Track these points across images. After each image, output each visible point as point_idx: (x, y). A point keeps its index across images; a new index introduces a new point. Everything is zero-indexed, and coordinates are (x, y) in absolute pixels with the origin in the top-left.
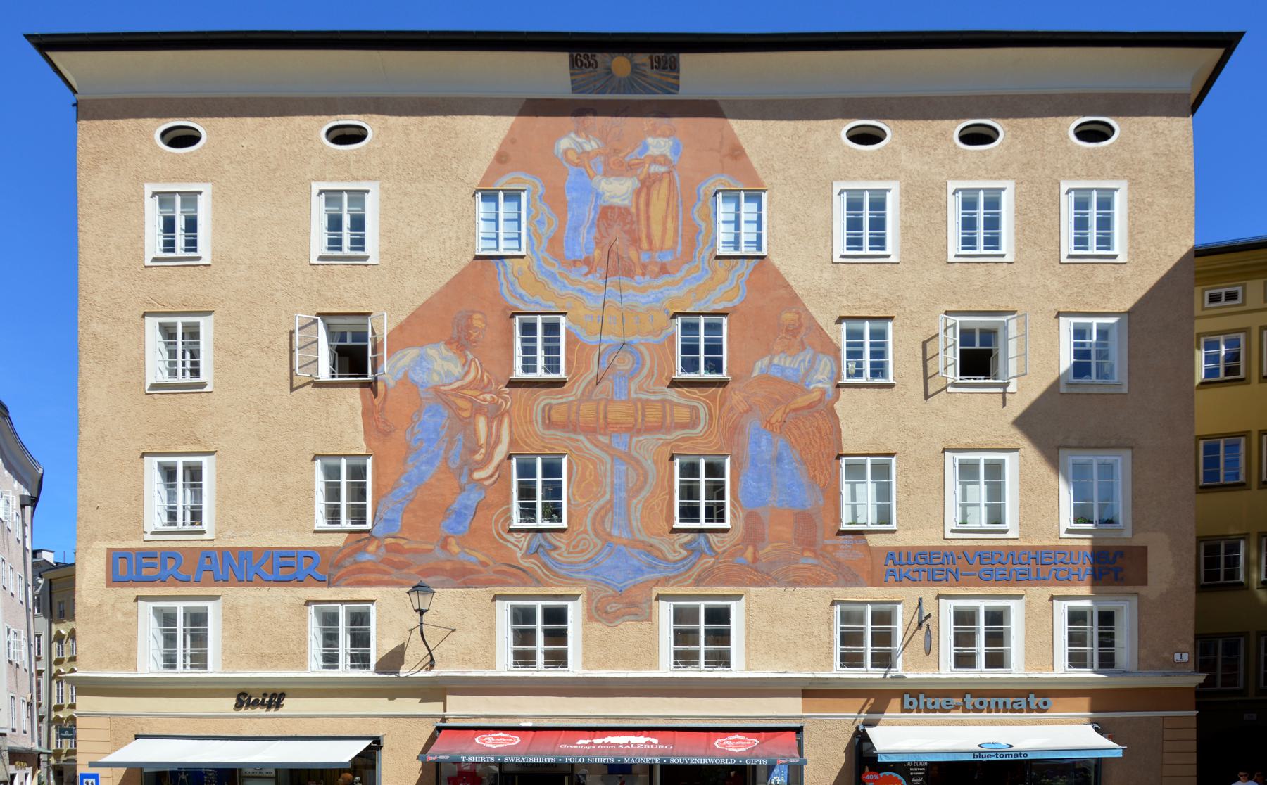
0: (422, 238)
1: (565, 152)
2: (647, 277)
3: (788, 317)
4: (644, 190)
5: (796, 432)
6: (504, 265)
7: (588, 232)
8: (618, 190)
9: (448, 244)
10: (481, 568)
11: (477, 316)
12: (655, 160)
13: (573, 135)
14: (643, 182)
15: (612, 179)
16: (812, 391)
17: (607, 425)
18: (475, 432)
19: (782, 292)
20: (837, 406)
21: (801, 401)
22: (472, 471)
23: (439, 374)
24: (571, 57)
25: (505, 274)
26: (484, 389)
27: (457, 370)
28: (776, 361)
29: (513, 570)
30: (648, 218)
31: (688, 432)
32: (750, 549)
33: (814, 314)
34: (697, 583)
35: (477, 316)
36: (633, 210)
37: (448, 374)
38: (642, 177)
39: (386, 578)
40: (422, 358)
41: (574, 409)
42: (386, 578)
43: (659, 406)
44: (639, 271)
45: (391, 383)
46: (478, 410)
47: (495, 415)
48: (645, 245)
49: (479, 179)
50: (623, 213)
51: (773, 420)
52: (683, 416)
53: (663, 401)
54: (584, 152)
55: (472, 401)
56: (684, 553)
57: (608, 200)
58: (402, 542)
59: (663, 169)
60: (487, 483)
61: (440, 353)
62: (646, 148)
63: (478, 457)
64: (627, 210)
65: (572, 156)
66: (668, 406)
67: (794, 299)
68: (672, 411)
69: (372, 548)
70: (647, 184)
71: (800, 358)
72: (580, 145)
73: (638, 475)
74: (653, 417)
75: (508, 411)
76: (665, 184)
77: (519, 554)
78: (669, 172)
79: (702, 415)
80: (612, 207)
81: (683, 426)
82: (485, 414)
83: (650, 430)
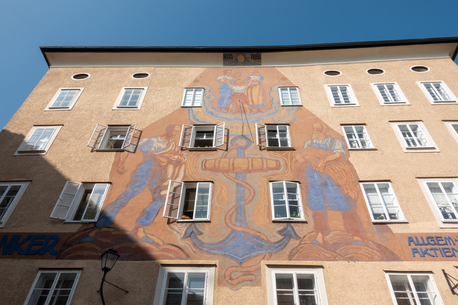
0: (160, 102)
1: (220, 79)
2: (252, 113)
3: (316, 125)
5: (332, 171)
6: (192, 110)
7: (228, 100)
9: (170, 104)
11: (177, 126)
12: (253, 81)
16: (335, 153)
17: (234, 168)
18: (166, 172)
19: (311, 117)
20: (350, 159)
21: (331, 158)
22: (161, 191)
23: (155, 148)
25: (192, 113)
26: (175, 154)
28: (314, 141)
29: (173, 248)
30: (252, 96)
31: (276, 172)
32: (320, 235)
34: (290, 257)
36: (246, 94)
39: (94, 253)
41: (218, 161)
42: (94, 253)
43: (260, 160)
47: (178, 164)
48: (251, 103)
50: (241, 95)
51: (319, 166)
52: (273, 164)
53: (262, 158)
54: (227, 79)
56: (280, 237)
62: (250, 78)
64: (243, 94)
65: (223, 80)
66: (264, 160)
67: (317, 120)
68: (266, 162)
69: (92, 234)
71: (326, 140)
74: (257, 164)
75: (185, 163)
77: (179, 237)
79: (282, 164)
80: (237, 93)
81: (273, 169)
82: (173, 164)
83: (256, 170)
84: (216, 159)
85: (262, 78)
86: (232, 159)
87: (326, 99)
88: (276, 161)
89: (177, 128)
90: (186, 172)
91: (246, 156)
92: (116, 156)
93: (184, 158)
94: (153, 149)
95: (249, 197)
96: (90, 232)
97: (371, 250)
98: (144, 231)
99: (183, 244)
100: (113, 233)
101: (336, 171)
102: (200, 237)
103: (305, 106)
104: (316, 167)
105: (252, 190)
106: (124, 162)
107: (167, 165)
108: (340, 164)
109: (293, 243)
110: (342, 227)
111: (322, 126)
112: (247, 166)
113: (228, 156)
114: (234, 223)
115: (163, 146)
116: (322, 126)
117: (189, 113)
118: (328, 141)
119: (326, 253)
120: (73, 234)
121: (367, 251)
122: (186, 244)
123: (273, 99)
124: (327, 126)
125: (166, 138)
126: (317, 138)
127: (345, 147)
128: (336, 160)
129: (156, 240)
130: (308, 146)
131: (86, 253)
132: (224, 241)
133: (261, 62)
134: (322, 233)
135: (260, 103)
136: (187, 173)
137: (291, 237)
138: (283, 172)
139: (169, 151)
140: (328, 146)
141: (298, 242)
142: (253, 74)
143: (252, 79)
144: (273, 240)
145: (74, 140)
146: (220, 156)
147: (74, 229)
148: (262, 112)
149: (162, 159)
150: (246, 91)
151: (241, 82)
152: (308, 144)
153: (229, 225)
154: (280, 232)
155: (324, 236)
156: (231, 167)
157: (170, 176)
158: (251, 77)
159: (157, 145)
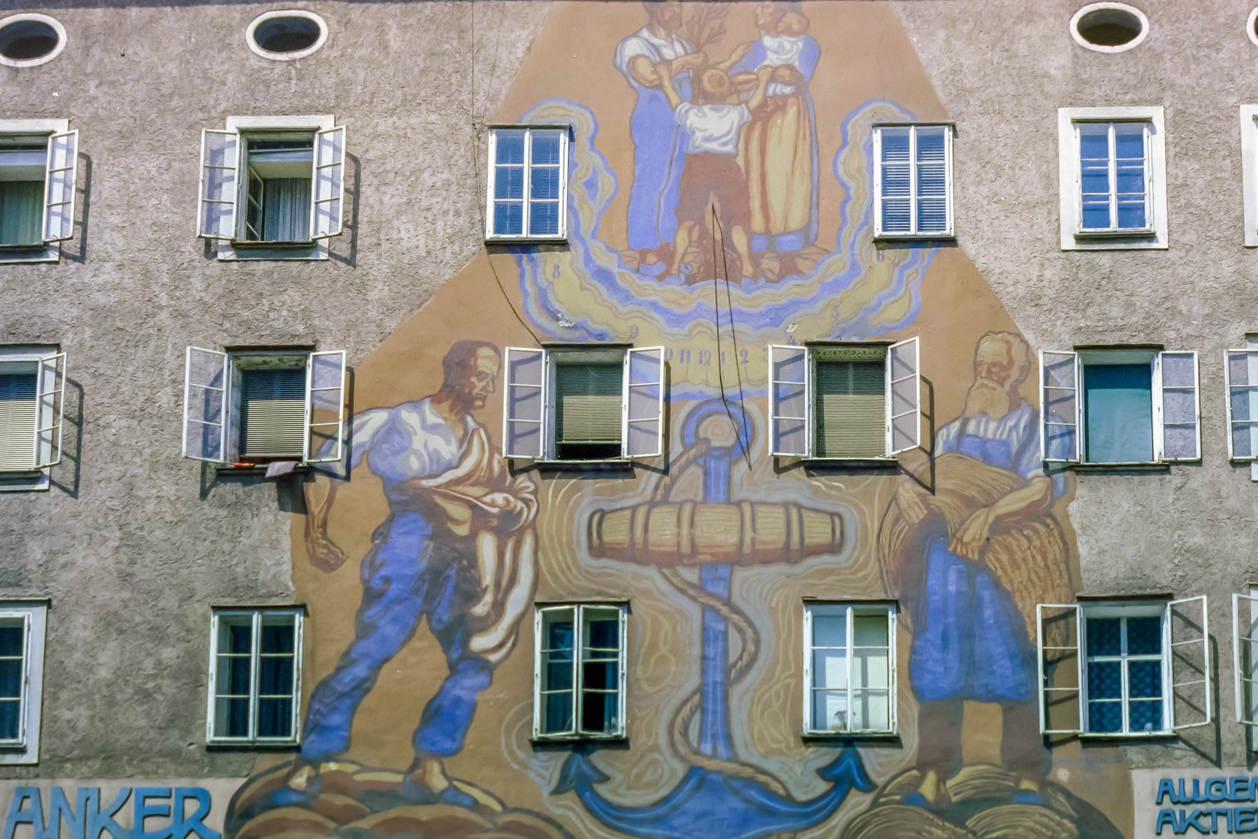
1: (633, 60)
2: (761, 281)
3: (991, 349)
4: (759, 124)
8: (713, 127)
9: (440, 224)
13: (645, 33)
15: (706, 108)
18: (474, 562)
21: (1011, 503)
26: (494, 485)
27: (448, 449)
28: (971, 428)
30: (763, 177)
32: (931, 777)
35: (484, 352)
37: (435, 456)
38: (754, 103)
40: (393, 429)
43: (780, 512)
44: (748, 269)
48: (758, 224)
51: (966, 539)
53: (786, 505)
55: (473, 507)
56: (822, 787)
57: (699, 143)
58: (350, 768)
59: (788, 90)
60: (494, 658)
63: (480, 609)
64: (726, 161)
65: (644, 68)
70: (763, 115)
71: (1011, 423)
72: (657, 49)
73: (744, 641)
75: (533, 525)
76: (792, 111)
77: (545, 793)
83: (764, 558)
84: (634, 509)
85: (813, 54)
86: (687, 509)
87: (1052, 201)
89: (484, 359)
90: (541, 562)
91: (737, 495)
93: (527, 502)
95: (741, 658)
96: (289, 776)
97: (1057, 818)
98: (443, 772)
99: (559, 811)
100: (358, 778)
101: (1019, 556)
102: (602, 790)
104: (960, 540)
105: (749, 633)
106: (324, 524)
107: (473, 536)
108: (1037, 532)
110: (995, 753)
111: (1009, 351)
112: (734, 540)
113: (673, 496)
114: (695, 744)
115: (448, 449)
116: (1009, 351)
117: (522, 276)
118: (1016, 426)
119: (938, 827)
121: (1045, 820)
123: (846, 200)
125: (452, 409)
126: (984, 413)
129: (483, 799)
134: (938, 773)
135: (796, 222)
136: (544, 569)
137: (853, 784)
138: (850, 562)
139: (468, 476)
140: (1015, 446)
141: (868, 799)
142: (774, 29)
143: (772, 59)
145: (124, 423)
146: (648, 495)
148: (799, 273)
150: (741, 146)
151: (720, 82)
152: (946, 442)
153: (682, 749)
154: (823, 773)
155: (941, 780)
158: (768, 41)
159: (425, 445)
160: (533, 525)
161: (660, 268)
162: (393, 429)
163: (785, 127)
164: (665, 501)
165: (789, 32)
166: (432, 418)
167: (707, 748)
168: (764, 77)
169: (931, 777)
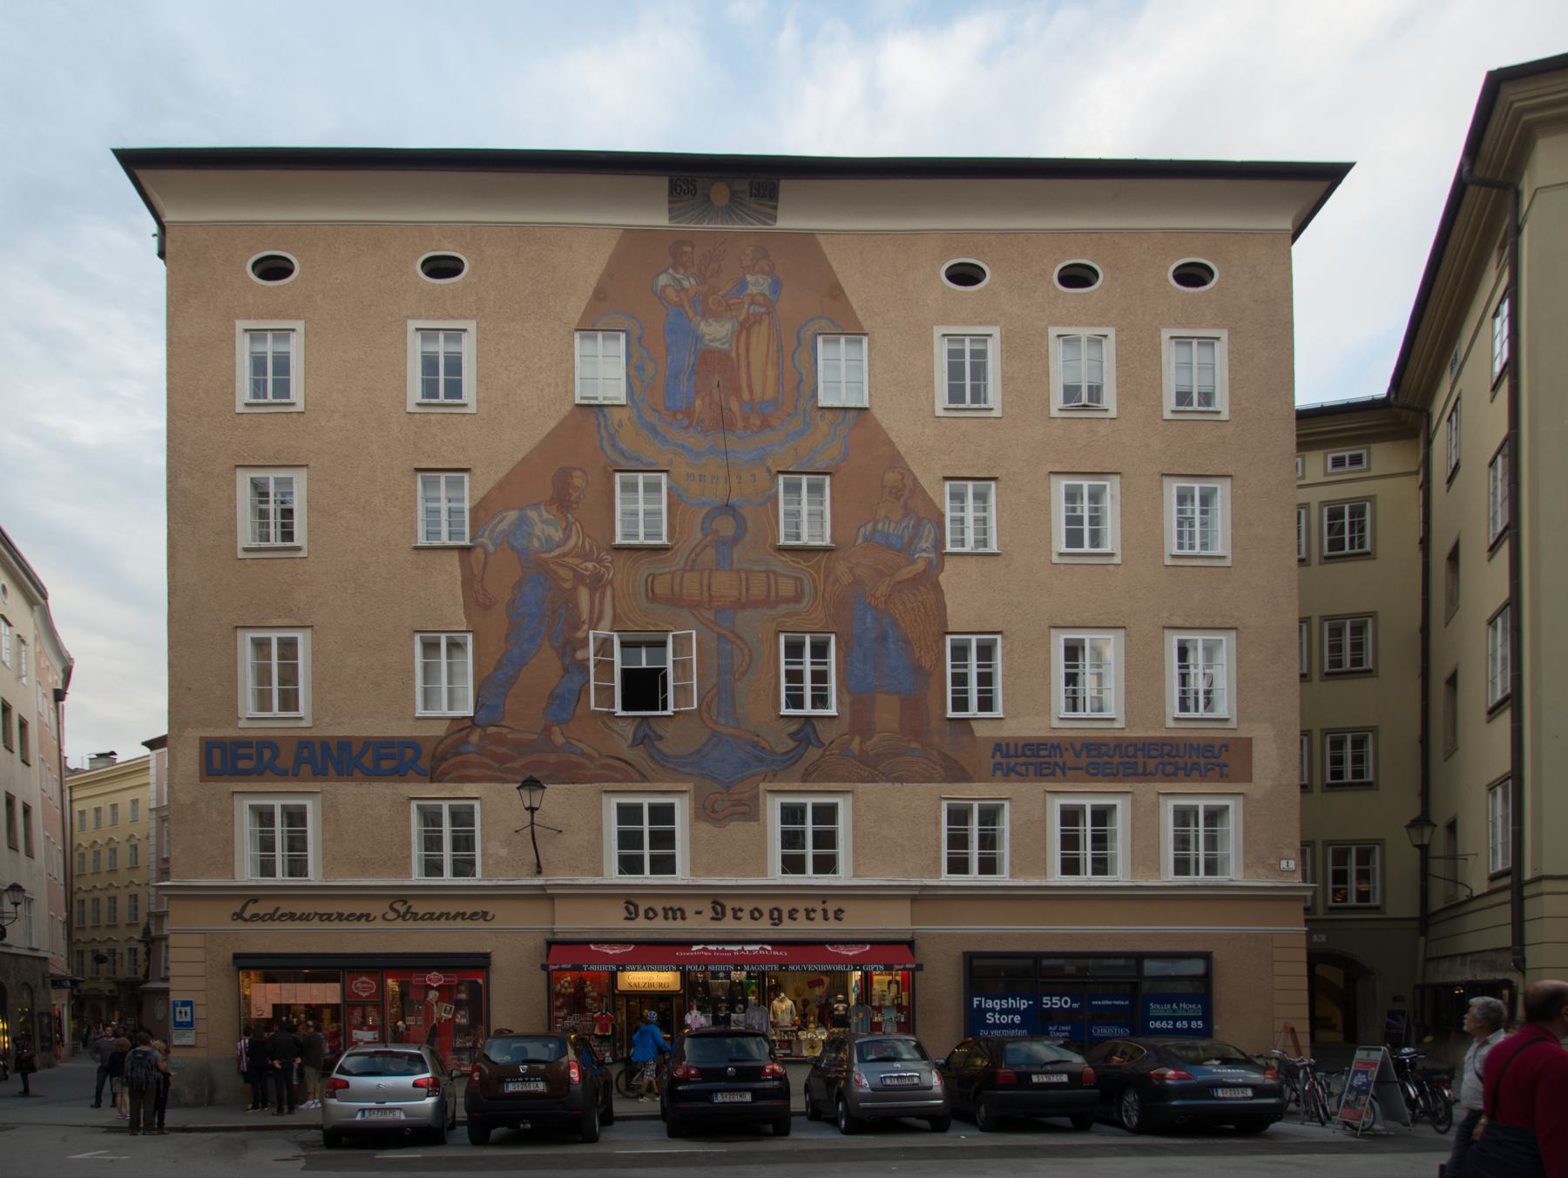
3: (892, 477)
4: (744, 334)
8: (716, 332)
10: (582, 760)
14: (742, 325)
16: (914, 562)
18: (576, 606)
21: (906, 573)
22: (575, 650)
23: (539, 539)
24: (671, 181)
26: (586, 557)
27: (558, 535)
28: (880, 527)
29: (617, 763)
30: (748, 365)
32: (857, 739)
33: (918, 475)
34: (805, 778)
35: (577, 473)
37: (549, 539)
38: (741, 318)
40: (522, 520)
41: (678, 579)
44: (740, 424)
45: (491, 549)
46: (579, 578)
48: (746, 396)
49: (578, 317)
52: (787, 588)
53: (767, 572)
54: (683, 289)
55: (574, 570)
56: (791, 744)
58: (505, 731)
59: (762, 310)
61: (540, 515)
62: (743, 284)
65: (671, 294)
69: (474, 738)
70: (746, 327)
75: (611, 583)
76: (766, 323)
78: (768, 313)
79: (807, 588)
81: (788, 600)
84: (673, 574)
85: (777, 286)
86: (706, 573)
88: (797, 579)
92: (462, 561)
93: (607, 568)
94: (536, 544)
96: (468, 735)
102: (659, 745)
103: (877, 413)
107: (574, 589)
109: (813, 753)
112: (736, 593)
115: (558, 535)
120: (442, 740)
122: (637, 756)
123: (801, 381)
124: (915, 479)
127: (940, 542)
128: (916, 579)
129: (587, 750)
130: (866, 539)
131: (474, 772)
132: (698, 752)
133: (775, 208)
135: (770, 394)
137: (810, 743)
143: (752, 289)
144: (781, 749)
147: (440, 730)
148: (770, 427)
149: (563, 572)
154: (792, 735)
155: (862, 742)
156: (706, 594)
157: (585, 616)
158: (749, 278)
160: (611, 583)
161: (686, 422)
162: (522, 520)
163: (761, 333)
164: (692, 569)
165: (762, 272)
166: (545, 515)
167: (722, 721)
168: (747, 300)
169: (857, 739)
